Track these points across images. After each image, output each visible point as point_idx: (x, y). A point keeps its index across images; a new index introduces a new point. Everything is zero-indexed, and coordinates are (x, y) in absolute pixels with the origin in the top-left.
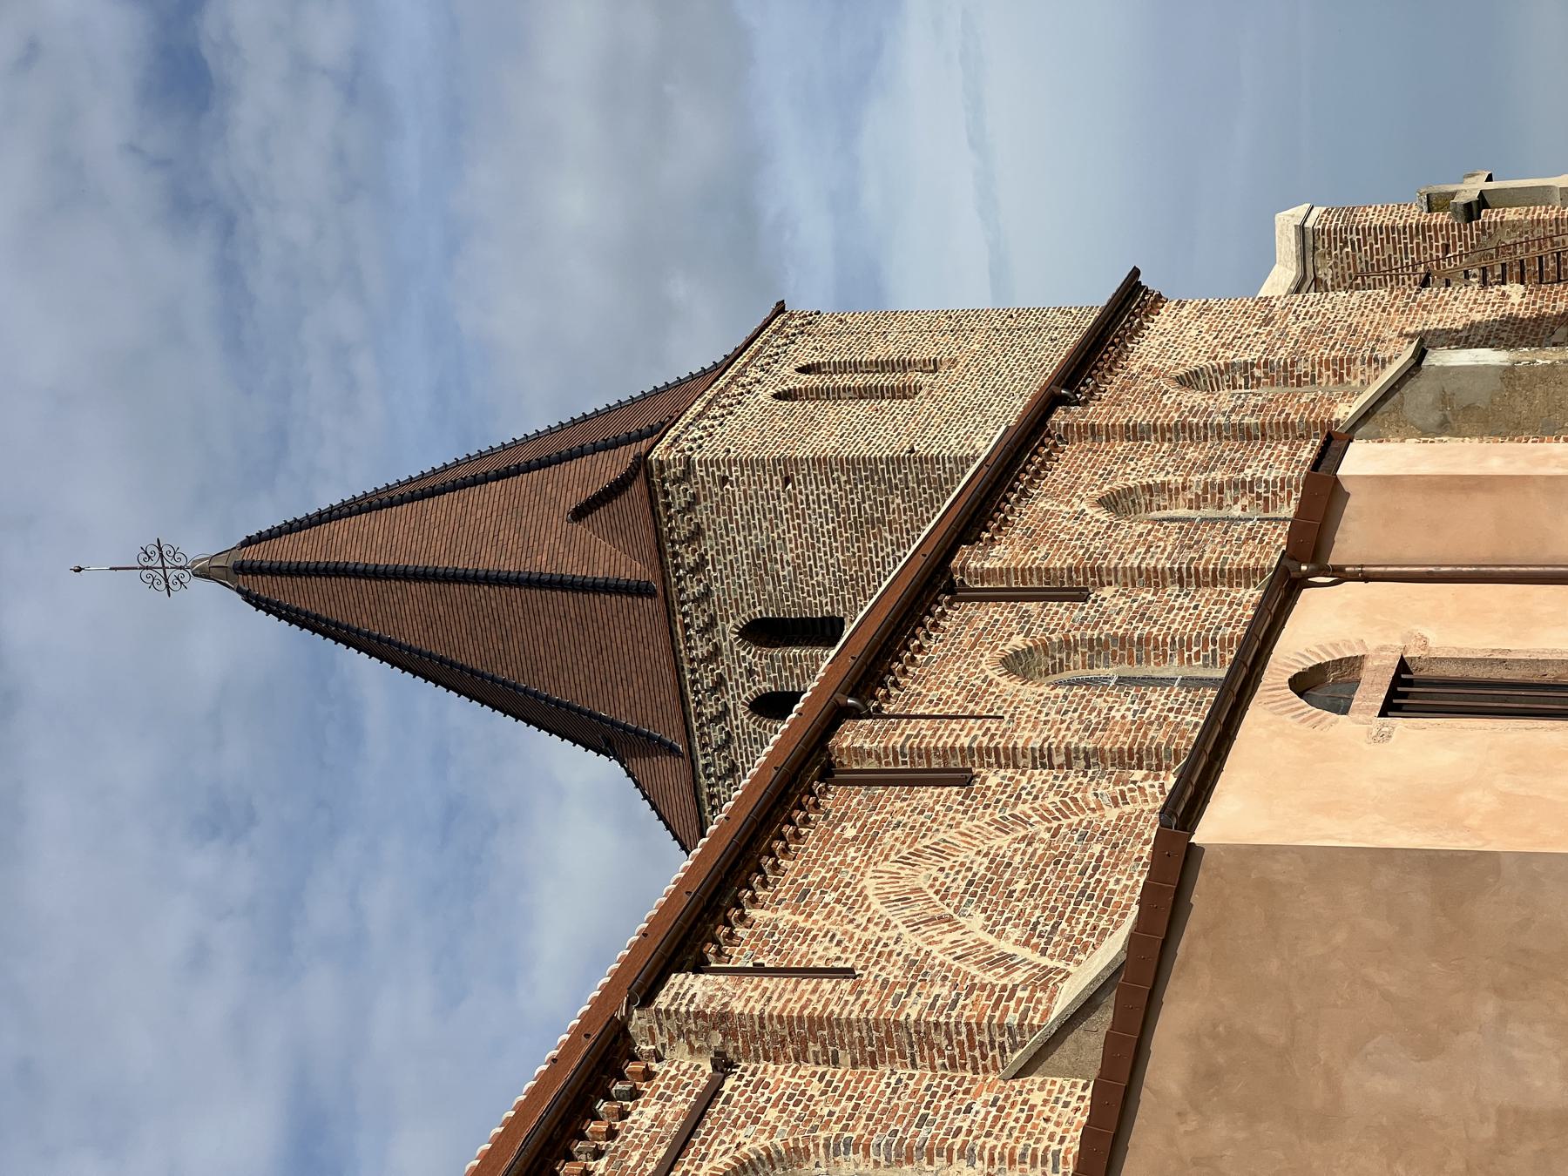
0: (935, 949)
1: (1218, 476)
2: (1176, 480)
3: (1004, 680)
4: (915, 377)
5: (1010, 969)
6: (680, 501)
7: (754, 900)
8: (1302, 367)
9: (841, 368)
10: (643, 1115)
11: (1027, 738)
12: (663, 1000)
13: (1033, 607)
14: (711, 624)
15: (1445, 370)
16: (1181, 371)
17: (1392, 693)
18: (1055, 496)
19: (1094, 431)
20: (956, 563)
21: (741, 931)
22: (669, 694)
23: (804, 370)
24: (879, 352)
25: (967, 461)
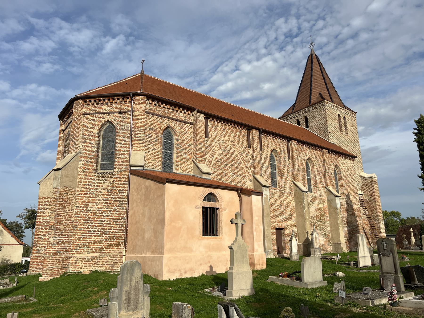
0: (215, 147)
1: (316, 172)
2: (315, 167)
3: (270, 149)
4: (344, 132)
5: (211, 157)
6: (320, 105)
7: (222, 123)
8: (341, 181)
9: (345, 123)
10: (182, 115)
11: (257, 154)
12: (199, 114)
13: (286, 151)
14: (306, 112)
15: (335, 200)
16: (338, 165)
17: (207, 208)
18: (310, 151)
19: (323, 155)
20: (293, 141)
21: (216, 122)
22: (298, 109)
23: (344, 117)
24: (348, 126)
25: (329, 140)
